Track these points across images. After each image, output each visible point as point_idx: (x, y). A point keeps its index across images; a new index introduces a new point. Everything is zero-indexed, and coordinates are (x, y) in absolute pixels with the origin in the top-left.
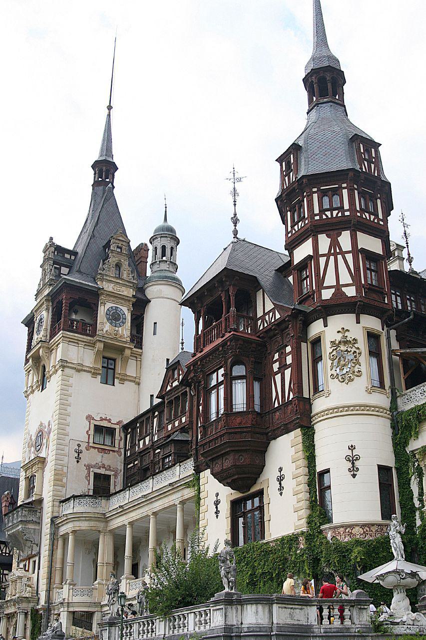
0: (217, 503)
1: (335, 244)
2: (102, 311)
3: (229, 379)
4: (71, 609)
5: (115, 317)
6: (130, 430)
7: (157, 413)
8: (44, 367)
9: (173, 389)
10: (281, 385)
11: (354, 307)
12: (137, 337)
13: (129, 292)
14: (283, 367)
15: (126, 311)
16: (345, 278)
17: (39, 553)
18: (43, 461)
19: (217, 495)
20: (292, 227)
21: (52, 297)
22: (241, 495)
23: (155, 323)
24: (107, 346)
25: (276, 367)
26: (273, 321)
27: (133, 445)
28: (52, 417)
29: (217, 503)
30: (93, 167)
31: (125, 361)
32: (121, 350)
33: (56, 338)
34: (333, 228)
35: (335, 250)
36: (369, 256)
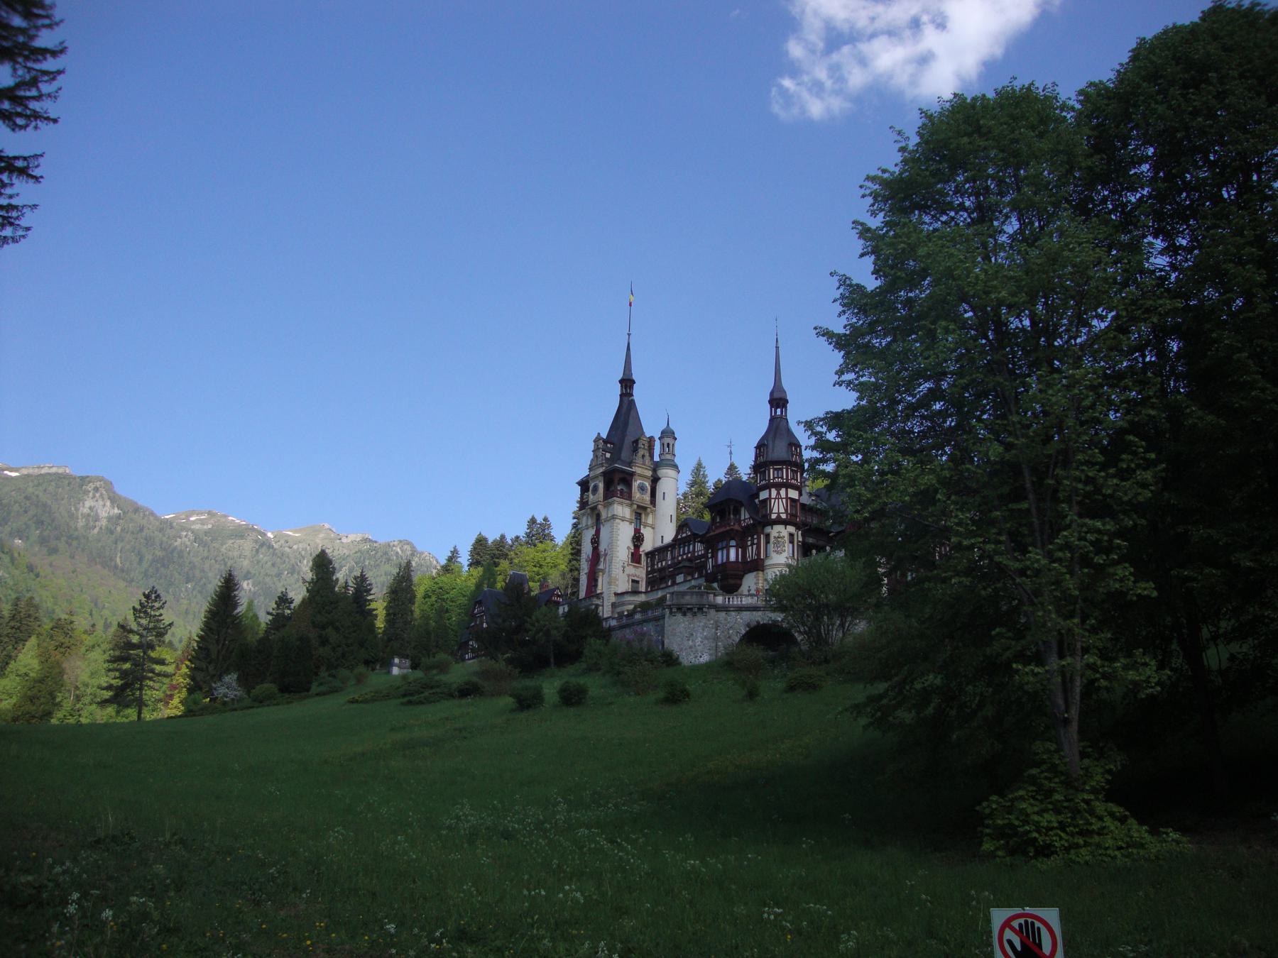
1: (778, 493)
2: (636, 483)
3: (728, 548)
5: (642, 488)
8: (598, 516)
11: (785, 523)
12: (653, 502)
13: (649, 473)
14: (752, 544)
15: (648, 485)
16: (782, 510)
21: (604, 474)
24: (639, 507)
27: (653, 565)
30: (621, 382)
31: (647, 515)
32: (645, 508)
34: (778, 486)
35: (778, 497)
36: (793, 500)
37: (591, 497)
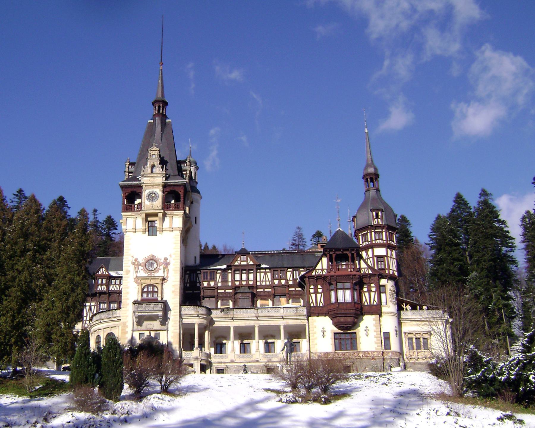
0: (323, 332)
1: (391, 254)
4: (202, 363)
6: (188, 272)
7: (219, 271)
9: (240, 265)
10: (369, 297)
17: (167, 330)
18: (164, 279)
19: (323, 328)
20: (376, 240)
22: (342, 331)
23: (196, 218)
25: (365, 289)
26: (367, 272)
28: (170, 256)
29: (323, 332)
33: (175, 212)
37: (146, 203)
